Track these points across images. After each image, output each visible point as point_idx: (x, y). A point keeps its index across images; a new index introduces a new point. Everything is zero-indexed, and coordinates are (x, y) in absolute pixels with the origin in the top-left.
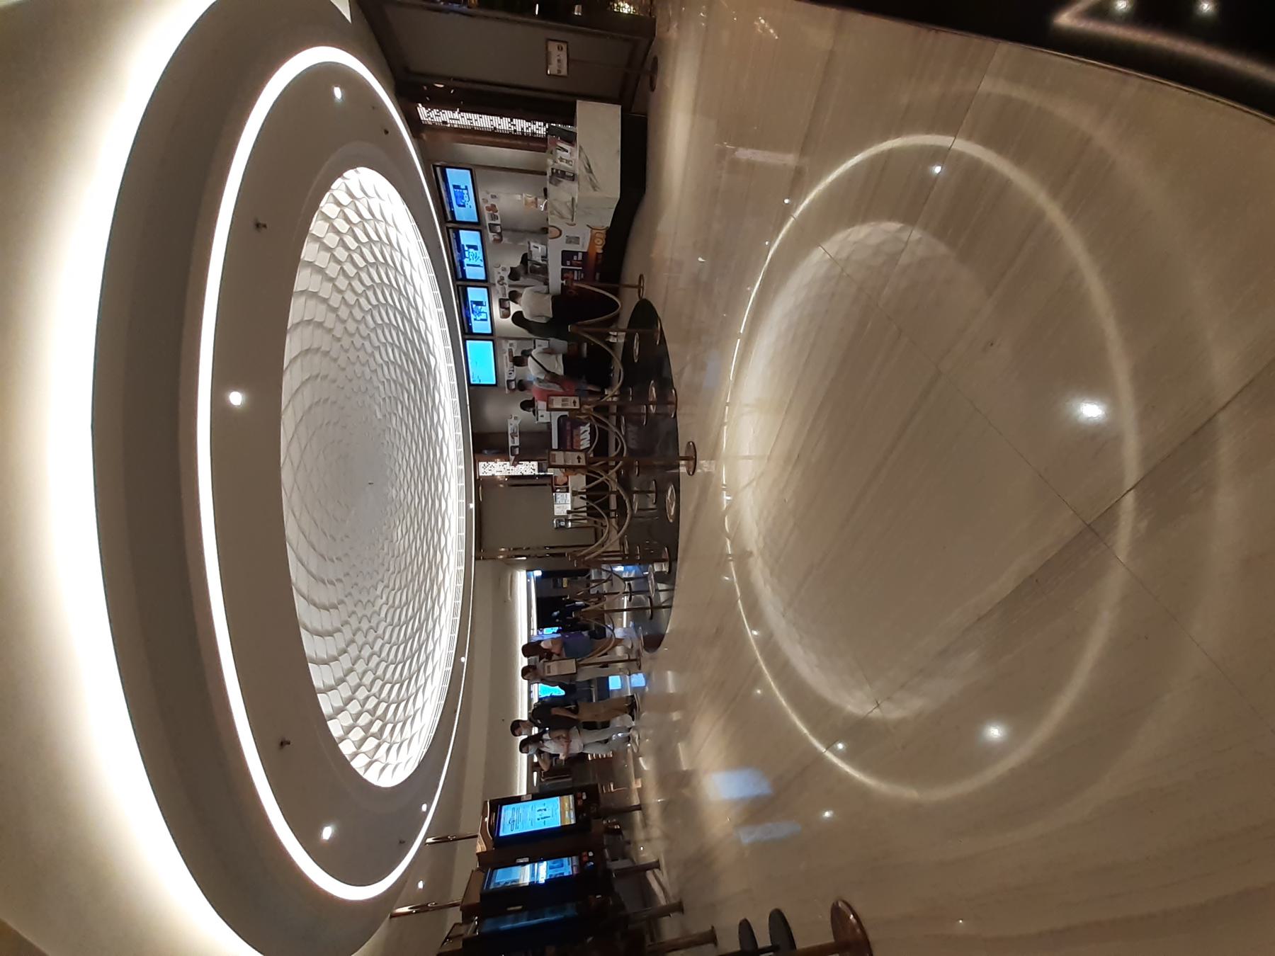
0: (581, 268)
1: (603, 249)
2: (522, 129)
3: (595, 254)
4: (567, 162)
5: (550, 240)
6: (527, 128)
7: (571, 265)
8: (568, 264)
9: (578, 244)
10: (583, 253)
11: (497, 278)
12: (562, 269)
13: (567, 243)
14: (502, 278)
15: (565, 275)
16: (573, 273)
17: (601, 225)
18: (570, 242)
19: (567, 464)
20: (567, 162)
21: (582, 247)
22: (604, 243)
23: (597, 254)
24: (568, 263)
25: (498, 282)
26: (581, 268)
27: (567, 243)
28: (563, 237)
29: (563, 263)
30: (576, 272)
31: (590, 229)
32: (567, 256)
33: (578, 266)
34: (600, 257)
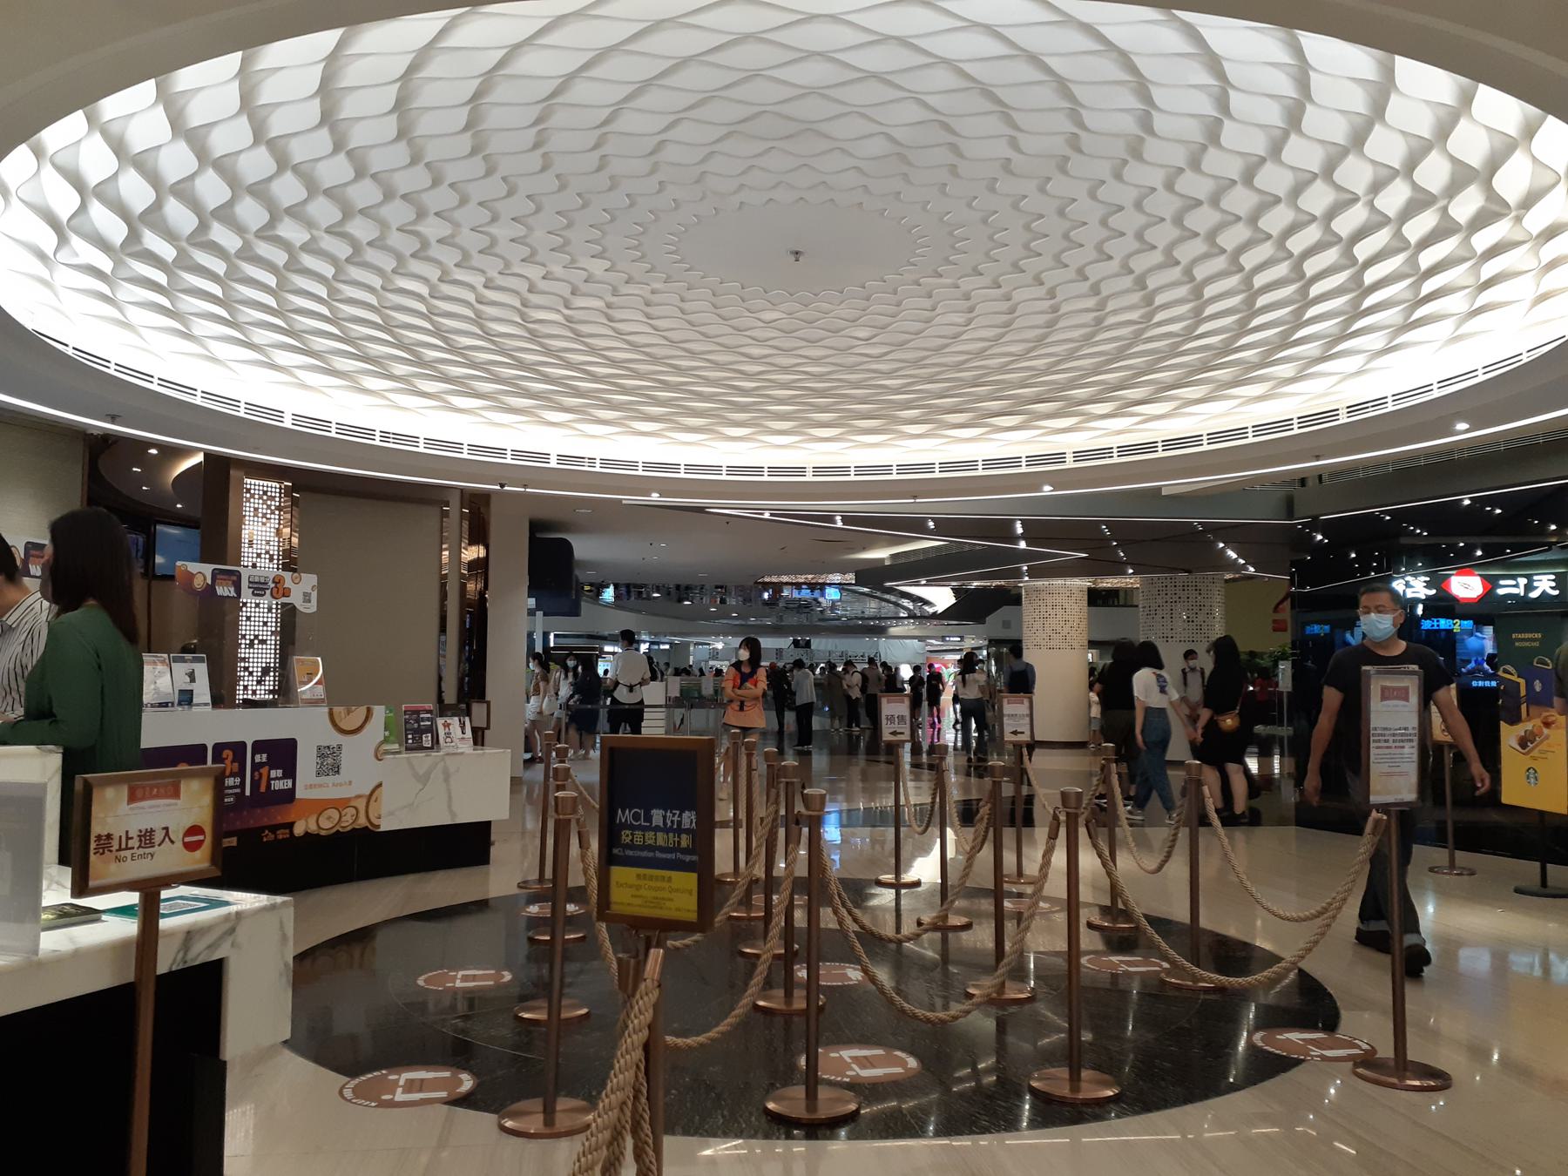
0: (248, 793)
1: (307, 834)
2: (243, 659)
5: (326, 710)
6: (246, 669)
7: (255, 767)
8: (258, 758)
10: (293, 790)
12: (243, 744)
15: (228, 753)
18: (321, 756)
19: (1005, 719)
20: (448, 735)
21: (308, 782)
22: (323, 833)
23: (290, 826)
24: (262, 758)
26: (248, 793)
28: (334, 739)
29: (259, 746)
30: (238, 780)
31: (368, 793)
32: (282, 753)
33: (255, 784)
34: (282, 834)
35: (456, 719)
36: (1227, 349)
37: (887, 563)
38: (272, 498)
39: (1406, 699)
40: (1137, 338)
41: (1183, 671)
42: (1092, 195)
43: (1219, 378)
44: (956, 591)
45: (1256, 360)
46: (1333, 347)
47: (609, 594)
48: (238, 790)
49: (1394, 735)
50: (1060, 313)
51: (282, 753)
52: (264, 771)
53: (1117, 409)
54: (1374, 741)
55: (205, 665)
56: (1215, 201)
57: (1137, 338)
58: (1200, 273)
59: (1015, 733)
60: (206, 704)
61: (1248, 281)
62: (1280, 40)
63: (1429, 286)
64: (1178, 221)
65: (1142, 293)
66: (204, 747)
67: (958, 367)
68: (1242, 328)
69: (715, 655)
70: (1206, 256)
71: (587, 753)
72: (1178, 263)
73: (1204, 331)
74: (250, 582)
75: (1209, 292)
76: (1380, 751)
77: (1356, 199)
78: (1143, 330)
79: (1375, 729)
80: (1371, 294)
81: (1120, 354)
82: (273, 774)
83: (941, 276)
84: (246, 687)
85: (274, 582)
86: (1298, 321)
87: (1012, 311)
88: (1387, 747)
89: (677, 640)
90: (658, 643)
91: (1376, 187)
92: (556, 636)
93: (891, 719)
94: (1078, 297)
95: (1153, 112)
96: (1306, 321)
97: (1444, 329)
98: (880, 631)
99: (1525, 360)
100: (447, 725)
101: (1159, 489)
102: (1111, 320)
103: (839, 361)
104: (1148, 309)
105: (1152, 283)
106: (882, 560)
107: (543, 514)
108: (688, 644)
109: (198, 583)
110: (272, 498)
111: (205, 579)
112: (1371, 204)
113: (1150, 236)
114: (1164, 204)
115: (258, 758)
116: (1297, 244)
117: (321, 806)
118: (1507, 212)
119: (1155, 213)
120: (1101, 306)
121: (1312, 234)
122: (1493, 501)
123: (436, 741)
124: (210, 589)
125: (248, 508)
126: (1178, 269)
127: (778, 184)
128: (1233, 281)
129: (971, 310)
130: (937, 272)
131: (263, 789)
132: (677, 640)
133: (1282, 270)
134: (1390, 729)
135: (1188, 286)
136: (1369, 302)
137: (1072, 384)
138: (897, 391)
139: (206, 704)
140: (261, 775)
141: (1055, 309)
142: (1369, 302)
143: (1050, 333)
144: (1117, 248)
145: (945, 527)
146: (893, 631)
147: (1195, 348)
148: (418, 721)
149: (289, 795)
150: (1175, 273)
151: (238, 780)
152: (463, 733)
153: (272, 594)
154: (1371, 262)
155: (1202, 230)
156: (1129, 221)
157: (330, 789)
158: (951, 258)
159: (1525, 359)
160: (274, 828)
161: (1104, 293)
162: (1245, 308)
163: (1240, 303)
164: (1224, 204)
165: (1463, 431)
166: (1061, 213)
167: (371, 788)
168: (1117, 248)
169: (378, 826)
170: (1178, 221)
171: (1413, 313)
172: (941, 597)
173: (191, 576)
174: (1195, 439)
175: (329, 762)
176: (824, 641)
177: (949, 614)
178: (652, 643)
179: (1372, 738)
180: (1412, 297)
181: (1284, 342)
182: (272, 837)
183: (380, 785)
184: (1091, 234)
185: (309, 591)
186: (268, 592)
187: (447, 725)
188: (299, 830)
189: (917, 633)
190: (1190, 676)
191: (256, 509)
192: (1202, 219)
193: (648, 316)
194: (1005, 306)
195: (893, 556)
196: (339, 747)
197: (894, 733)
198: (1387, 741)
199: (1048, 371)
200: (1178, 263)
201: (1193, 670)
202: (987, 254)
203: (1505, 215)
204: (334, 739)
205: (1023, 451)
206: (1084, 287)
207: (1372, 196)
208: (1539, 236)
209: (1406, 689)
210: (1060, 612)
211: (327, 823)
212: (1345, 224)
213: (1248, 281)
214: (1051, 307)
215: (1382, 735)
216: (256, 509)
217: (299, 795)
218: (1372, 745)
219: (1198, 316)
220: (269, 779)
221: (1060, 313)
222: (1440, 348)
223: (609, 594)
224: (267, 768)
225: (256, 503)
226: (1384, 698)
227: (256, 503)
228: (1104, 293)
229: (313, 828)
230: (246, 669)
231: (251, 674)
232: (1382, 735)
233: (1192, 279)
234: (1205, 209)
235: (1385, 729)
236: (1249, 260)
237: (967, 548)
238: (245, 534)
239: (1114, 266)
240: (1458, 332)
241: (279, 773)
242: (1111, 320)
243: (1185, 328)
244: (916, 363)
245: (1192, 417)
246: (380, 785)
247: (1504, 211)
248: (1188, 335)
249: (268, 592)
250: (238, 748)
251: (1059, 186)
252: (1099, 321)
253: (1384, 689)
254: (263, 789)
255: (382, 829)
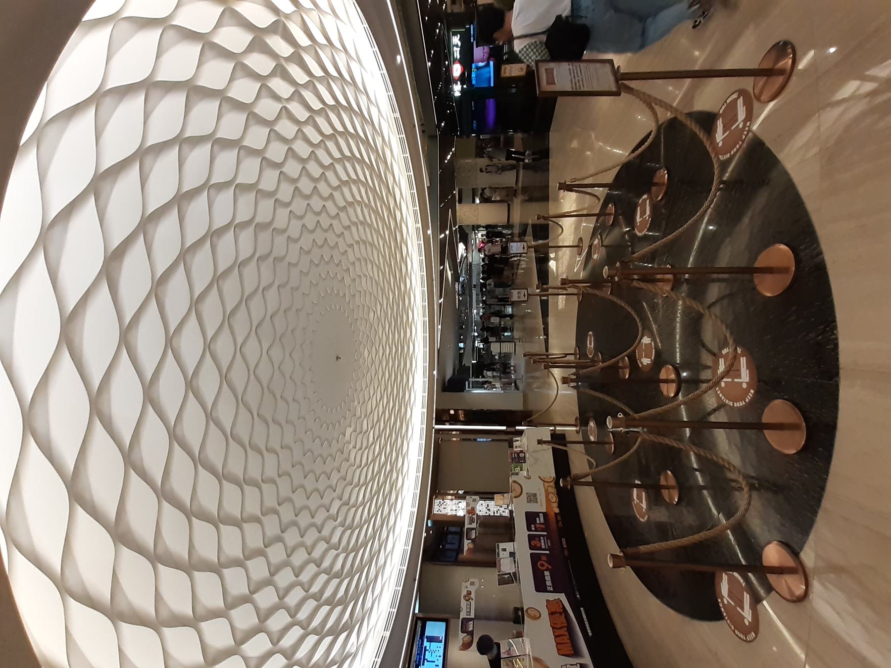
0: (545, 533)
1: (559, 507)
3: (553, 515)
4: (520, 447)
8: (533, 529)
9: (537, 502)
11: (464, 593)
12: (529, 535)
13: (528, 502)
14: (469, 593)
16: (540, 541)
17: (549, 476)
21: (540, 507)
22: (557, 500)
23: (556, 514)
25: (465, 597)
26: (545, 533)
27: (528, 502)
28: (524, 496)
29: (529, 529)
31: (542, 482)
34: (559, 518)
35: (514, 443)
36: (371, 167)
37: (452, 272)
38: (440, 503)
39: (553, 69)
40: (368, 206)
41: (487, 172)
42: (296, 241)
43: (384, 169)
44: (460, 242)
45: (375, 155)
46: (367, 120)
47: (461, 345)
48: (545, 537)
49: (574, 77)
50: (359, 240)
51: (531, 517)
52: (537, 526)
53: (398, 209)
54: (580, 89)
55: (500, 544)
56: (294, 181)
57: (368, 206)
58: (335, 182)
59: (524, 248)
60: (513, 544)
61: (338, 160)
62: (154, 161)
63: (333, 72)
64: (308, 197)
65: (347, 207)
66: (531, 554)
67: (384, 274)
68: (361, 161)
69: (478, 313)
70: (326, 181)
71: (512, 366)
72: (331, 194)
73: (364, 178)
74: (470, 524)
75: (344, 178)
76: (585, 86)
77: (286, 108)
78: (365, 204)
79: (572, 88)
80: (353, 108)
81: (376, 212)
82: (538, 522)
83: (345, 294)
84: (503, 512)
85: (469, 514)
86: (356, 136)
87: (359, 260)
88: (582, 80)
89: (474, 324)
90: (474, 330)
91: (276, 97)
92: (473, 360)
93: (519, 297)
94: (351, 234)
95: (237, 222)
96: (355, 132)
97: (354, 66)
98: (471, 264)
99: (367, 25)
100: (516, 447)
101: (428, 187)
102: (361, 218)
103: (378, 345)
104: (355, 204)
105: (342, 204)
106: (451, 274)
107: (440, 389)
108: (475, 321)
109: (471, 546)
110: (440, 503)
111: (469, 543)
112: (288, 100)
113: (317, 209)
114: (299, 206)
115: (533, 529)
116: (316, 138)
117: (548, 500)
118: (281, 24)
119: (305, 209)
120: (355, 224)
121: (309, 131)
122: (429, 53)
123: (521, 452)
124: (473, 541)
125: (444, 512)
126: (335, 193)
127: (302, 383)
128: (338, 167)
129: (366, 260)
130: (343, 297)
131: (543, 526)
132: (474, 324)
133: (331, 145)
134: (571, 79)
135: (343, 188)
136: (344, 102)
137: (389, 228)
138: (394, 294)
139: (513, 544)
140: (539, 528)
141: (358, 243)
142: (344, 102)
143: (368, 241)
144: (325, 223)
145: (442, 263)
146: (471, 261)
147: (372, 182)
148: (515, 458)
149: (545, 514)
150: (337, 195)
151: (542, 538)
152: (518, 441)
153: (474, 515)
154: (322, 101)
155: (312, 185)
156: (310, 221)
157: (542, 497)
158: (339, 279)
159: (366, 25)
160: (557, 522)
161: (348, 223)
162: (351, 161)
163: (350, 163)
164: (296, 176)
165: (400, 58)
166: (308, 252)
167: (540, 480)
168: (325, 223)
169: (554, 478)
170: (308, 197)
171: (348, 81)
172: (461, 247)
173: (469, 549)
174: (409, 177)
175: (532, 498)
176: (473, 281)
177: (466, 244)
178: (474, 332)
179: (578, 90)
180: (340, 82)
181: (366, 142)
182: (560, 522)
183: (539, 477)
184: (319, 236)
185: (472, 499)
186: (473, 516)
187: (516, 447)
188: (557, 511)
189: (471, 253)
190: (488, 170)
191: (444, 508)
192: (306, 186)
193: (361, 449)
194: (357, 263)
195: (450, 270)
196: (527, 493)
197: (524, 295)
198: (579, 81)
199: (384, 239)
200: (331, 194)
201: (486, 169)
202: (337, 265)
203: (284, 25)
204: (524, 496)
205: (415, 242)
206: (346, 233)
207: (282, 100)
208: (296, 7)
209: (546, 70)
210: (466, 213)
211: (554, 499)
212: (302, 114)
213: (338, 160)
214: (356, 244)
215: (576, 84)
216: (444, 508)
217: (545, 511)
218: (582, 90)
219: (357, 182)
220: (540, 523)
221: (359, 240)
222: (364, 68)
223: (461, 345)
224: (536, 525)
225: (441, 508)
226: (554, 83)
227: (441, 508)
228: (348, 223)
229: (555, 505)
230: (497, 512)
231: (499, 510)
232: (576, 84)
233: (339, 186)
234: (299, 185)
235: (572, 81)
236: (327, 161)
237: (449, 255)
238: (450, 513)
239: (335, 223)
240: (355, 58)
241: (537, 519)
242: (361, 218)
243: (363, 186)
244: (383, 290)
245: (401, 181)
246: (539, 477)
247: (281, 24)
248: (366, 184)
249: (473, 516)
250: (531, 538)
251: (293, 257)
252: (362, 223)
253: (548, 83)
254: (543, 526)
255: (555, 476)
